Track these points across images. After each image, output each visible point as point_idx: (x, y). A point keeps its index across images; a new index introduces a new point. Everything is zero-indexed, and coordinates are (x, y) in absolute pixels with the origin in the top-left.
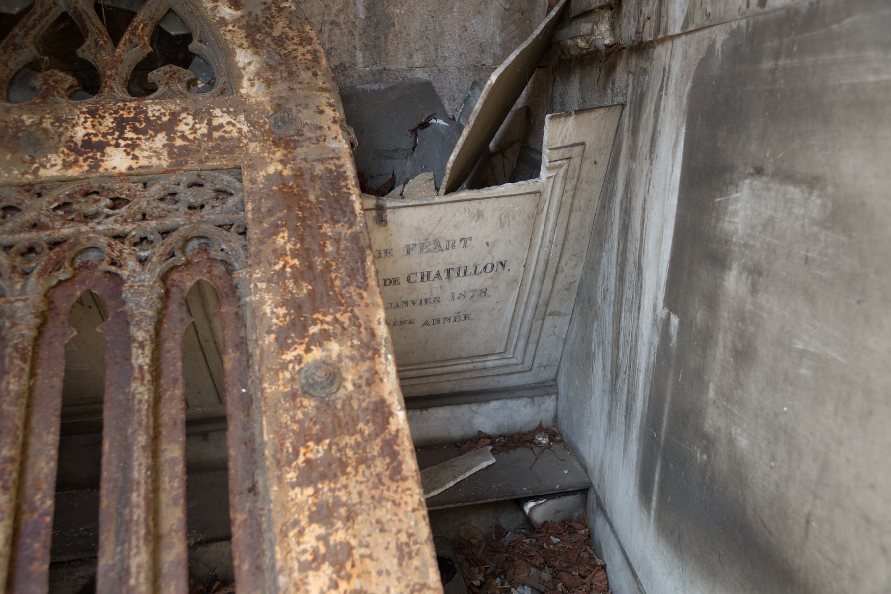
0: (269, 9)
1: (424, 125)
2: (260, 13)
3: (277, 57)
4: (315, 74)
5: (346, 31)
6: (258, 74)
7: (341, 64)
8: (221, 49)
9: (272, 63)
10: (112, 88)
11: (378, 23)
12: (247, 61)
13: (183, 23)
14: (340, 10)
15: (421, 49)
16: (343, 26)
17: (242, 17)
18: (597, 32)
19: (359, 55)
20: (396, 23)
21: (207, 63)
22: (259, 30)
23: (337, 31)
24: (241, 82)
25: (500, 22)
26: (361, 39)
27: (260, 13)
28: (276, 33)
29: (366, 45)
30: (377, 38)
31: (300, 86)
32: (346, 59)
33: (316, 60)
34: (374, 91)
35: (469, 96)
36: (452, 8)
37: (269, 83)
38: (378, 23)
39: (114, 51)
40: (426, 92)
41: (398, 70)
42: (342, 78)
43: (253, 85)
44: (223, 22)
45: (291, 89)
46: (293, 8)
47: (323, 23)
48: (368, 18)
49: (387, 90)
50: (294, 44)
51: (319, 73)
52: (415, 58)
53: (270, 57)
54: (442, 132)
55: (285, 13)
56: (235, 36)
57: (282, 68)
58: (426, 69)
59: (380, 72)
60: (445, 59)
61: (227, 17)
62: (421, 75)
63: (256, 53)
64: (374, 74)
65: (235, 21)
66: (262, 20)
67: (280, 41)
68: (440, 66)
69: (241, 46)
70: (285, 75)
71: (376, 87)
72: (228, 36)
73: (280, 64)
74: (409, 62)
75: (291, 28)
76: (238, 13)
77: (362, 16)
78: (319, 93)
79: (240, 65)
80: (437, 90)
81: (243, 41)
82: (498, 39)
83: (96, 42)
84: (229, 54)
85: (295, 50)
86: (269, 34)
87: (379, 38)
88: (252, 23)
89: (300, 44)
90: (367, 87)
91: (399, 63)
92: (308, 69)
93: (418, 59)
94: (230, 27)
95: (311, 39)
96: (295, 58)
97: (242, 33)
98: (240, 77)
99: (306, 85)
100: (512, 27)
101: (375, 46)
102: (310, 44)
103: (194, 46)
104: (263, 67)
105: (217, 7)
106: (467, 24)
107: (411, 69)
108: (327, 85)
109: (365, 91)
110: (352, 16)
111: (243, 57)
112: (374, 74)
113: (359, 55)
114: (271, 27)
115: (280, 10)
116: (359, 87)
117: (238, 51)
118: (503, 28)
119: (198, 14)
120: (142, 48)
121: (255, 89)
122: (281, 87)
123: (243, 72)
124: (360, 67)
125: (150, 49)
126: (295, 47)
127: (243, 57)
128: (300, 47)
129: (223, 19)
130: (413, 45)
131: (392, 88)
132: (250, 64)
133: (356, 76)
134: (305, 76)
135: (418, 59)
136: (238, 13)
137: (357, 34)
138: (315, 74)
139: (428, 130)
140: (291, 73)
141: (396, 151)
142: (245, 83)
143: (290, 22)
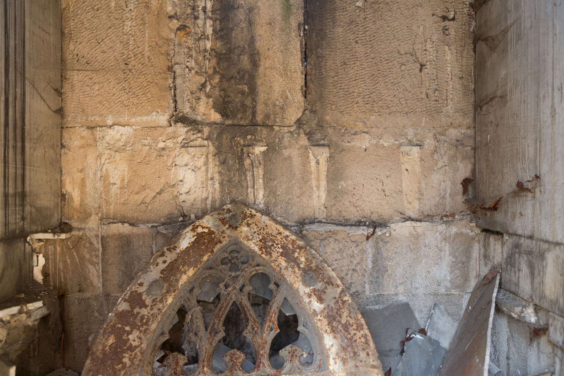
0: (337, 302)
1: (410, 339)
2: (333, 306)
3: (346, 341)
4: (368, 354)
5: (361, 274)
6: (337, 354)
7: (357, 291)
8: (316, 334)
9: (344, 345)
10: (264, 364)
11: (379, 270)
12: (331, 344)
13: (292, 308)
14: (358, 263)
15: (403, 283)
16: (359, 271)
17: (325, 308)
18: (525, 312)
19: (367, 286)
20: (389, 270)
21: (306, 338)
22: (334, 319)
23: (355, 274)
24: (329, 361)
25: (449, 269)
26: (368, 278)
27: (333, 306)
28: (343, 321)
29: (372, 282)
30: (378, 277)
31: (361, 364)
32: (360, 289)
33: (367, 343)
34: (376, 310)
35: (432, 314)
36: (421, 262)
37: (344, 361)
38: (379, 270)
39: (262, 335)
40: (406, 309)
41: (389, 295)
42: (357, 299)
43: (336, 363)
44: (315, 313)
45: (357, 366)
46: (350, 301)
47: (349, 270)
48: (373, 267)
49: (384, 309)
50: (354, 329)
51: (370, 353)
52: (399, 288)
53: (342, 341)
54: (420, 343)
55: (346, 305)
56: (322, 324)
57: (349, 349)
58: (405, 294)
59: (379, 296)
60: (417, 288)
61: (317, 309)
62: (402, 298)
63: (335, 337)
64: (375, 297)
65: (322, 312)
66: (335, 311)
67: (346, 327)
68: (413, 293)
69: (326, 332)
70: (352, 355)
71: (377, 307)
72: (319, 324)
73: (348, 346)
74: (396, 290)
75: (350, 317)
76: (322, 306)
77: (370, 267)
78: (372, 370)
79: (327, 347)
80: (411, 306)
81: (327, 327)
82: (449, 278)
83: (253, 329)
84: (321, 339)
85: (355, 334)
86: (339, 322)
87: (379, 277)
88: (330, 313)
89: (357, 330)
90: (372, 307)
91: (389, 290)
92: (364, 350)
93: (401, 289)
94: (319, 317)
95: (363, 325)
96: (356, 341)
97: (325, 322)
98: (328, 357)
99: (364, 363)
100: (457, 272)
101: (376, 282)
102: (362, 329)
103: (300, 328)
104: (339, 348)
105: (311, 301)
106: (430, 270)
107: (397, 294)
108: (375, 363)
109: (371, 310)
110: (364, 266)
111: (329, 341)
112: (375, 297)
113: (367, 286)
114: (340, 317)
115: (344, 302)
116: (367, 307)
117: (325, 335)
118: (452, 272)
119: (301, 306)
120: (275, 331)
121: (337, 366)
122: (351, 364)
123: (329, 353)
124: (367, 293)
125: (279, 331)
126: (355, 332)
127: (329, 341)
128: (357, 332)
129: (315, 310)
130: (398, 281)
131: (387, 308)
132: (332, 345)
133: (365, 298)
134: (363, 355)
135: (401, 289)
136: (322, 306)
137: (366, 275)
138: (368, 354)
139: (411, 341)
140: (355, 353)
141: (390, 351)
142: (331, 362)
143: (350, 313)
